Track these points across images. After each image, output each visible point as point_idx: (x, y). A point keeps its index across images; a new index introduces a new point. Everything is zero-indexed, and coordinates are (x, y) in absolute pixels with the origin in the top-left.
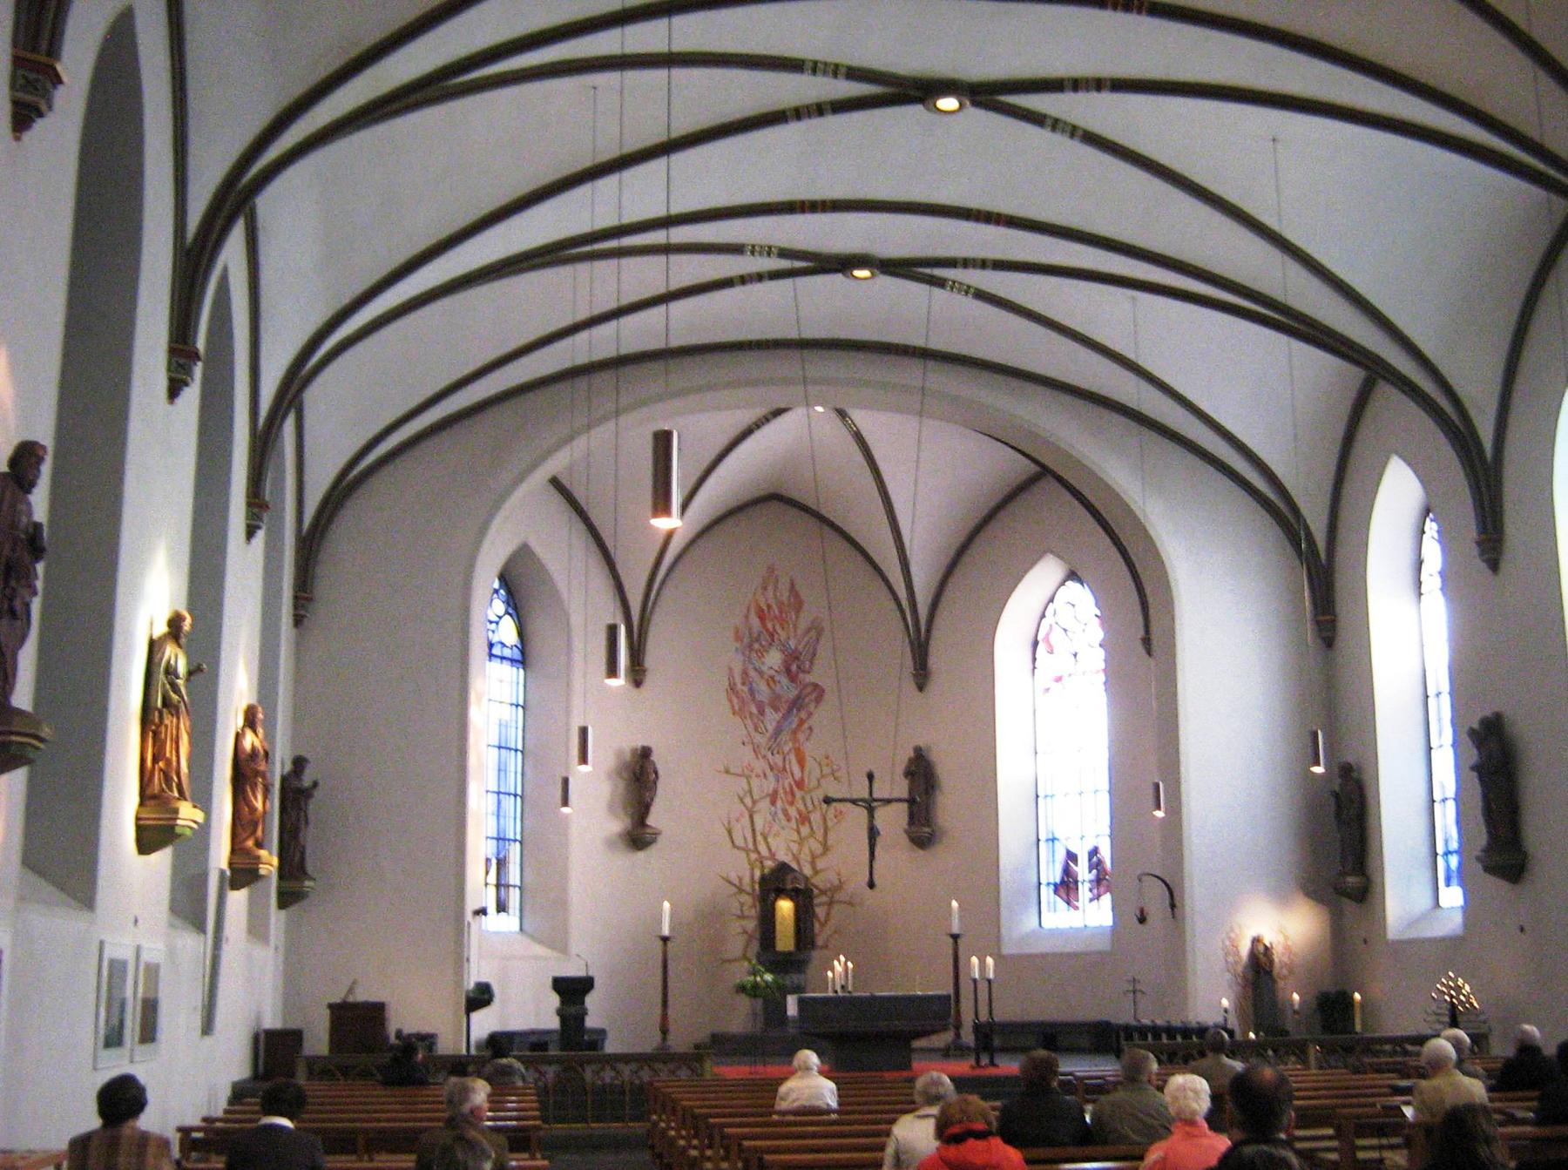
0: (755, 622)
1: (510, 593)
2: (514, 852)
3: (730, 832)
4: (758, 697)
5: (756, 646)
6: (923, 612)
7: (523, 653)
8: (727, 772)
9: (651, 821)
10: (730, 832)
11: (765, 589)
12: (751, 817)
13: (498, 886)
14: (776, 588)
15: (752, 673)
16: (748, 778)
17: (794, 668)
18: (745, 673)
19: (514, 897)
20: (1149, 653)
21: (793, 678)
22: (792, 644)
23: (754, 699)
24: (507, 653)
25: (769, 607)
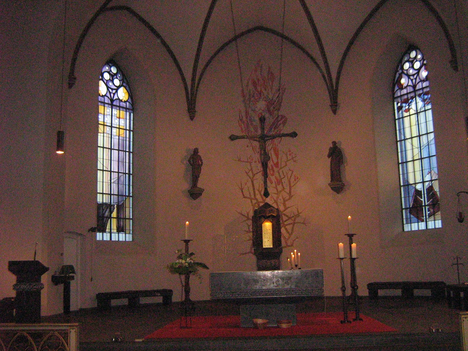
0: (251, 87)
1: (123, 75)
2: (129, 203)
3: (242, 190)
4: (254, 123)
5: (252, 99)
6: (334, 76)
7: (133, 104)
8: (239, 160)
9: (199, 185)
10: (242, 190)
11: (256, 71)
12: (252, 182)
13: (118, 218)
14: (261, 71)
15: (251, 112)
16: (250, 163)
17: (272, 108)
18: (247, 113)
19: (129, 225)
20: (456, 69)
21: (271, 113)
22: (270, 97)
23: (252, 124)
24: (123, 104)
25: (258, 80)
